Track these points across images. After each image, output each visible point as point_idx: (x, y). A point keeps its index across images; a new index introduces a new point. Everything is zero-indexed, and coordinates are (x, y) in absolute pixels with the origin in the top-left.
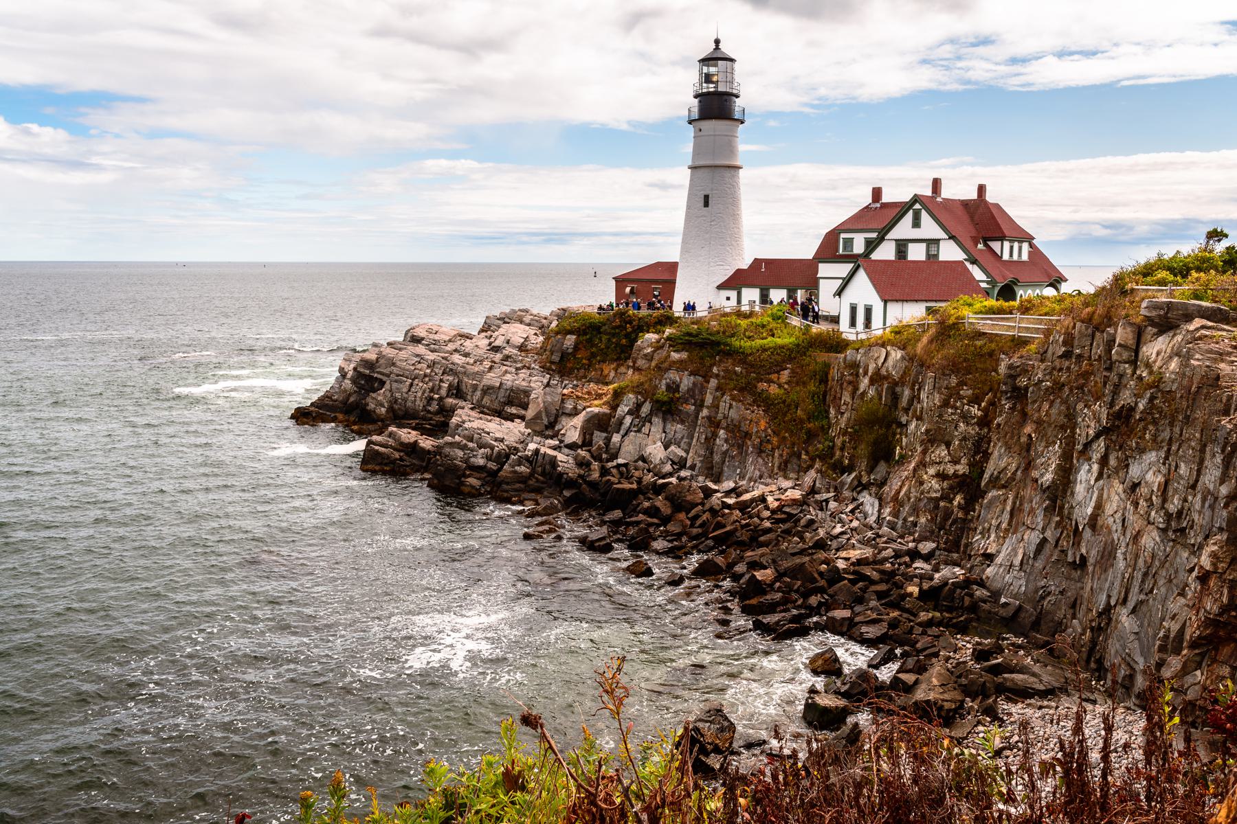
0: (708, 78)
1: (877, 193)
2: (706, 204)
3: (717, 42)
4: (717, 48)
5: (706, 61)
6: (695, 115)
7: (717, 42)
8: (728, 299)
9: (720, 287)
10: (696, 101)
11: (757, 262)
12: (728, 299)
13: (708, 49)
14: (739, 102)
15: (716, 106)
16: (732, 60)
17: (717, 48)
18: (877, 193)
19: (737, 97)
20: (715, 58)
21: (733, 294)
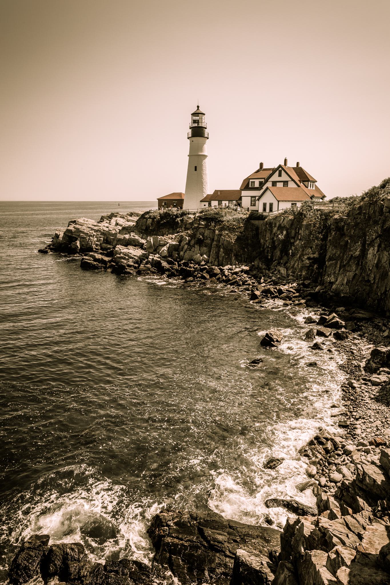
0: (195, 122)
1: (261, 165)
2: (196, 170)
3: (198, 107)
4: (198, 109)
5: (194, 114)
6: (190, 136)
7: (198, 107)
8: (205, 205)
10: (190, 130)
11: (216, 192)
12: (205, 205)
13: (194, 110)
15: (198, 132)
16: (204, 114)
17: (198, 109)
18: (261, 165)
19: (206, 128)
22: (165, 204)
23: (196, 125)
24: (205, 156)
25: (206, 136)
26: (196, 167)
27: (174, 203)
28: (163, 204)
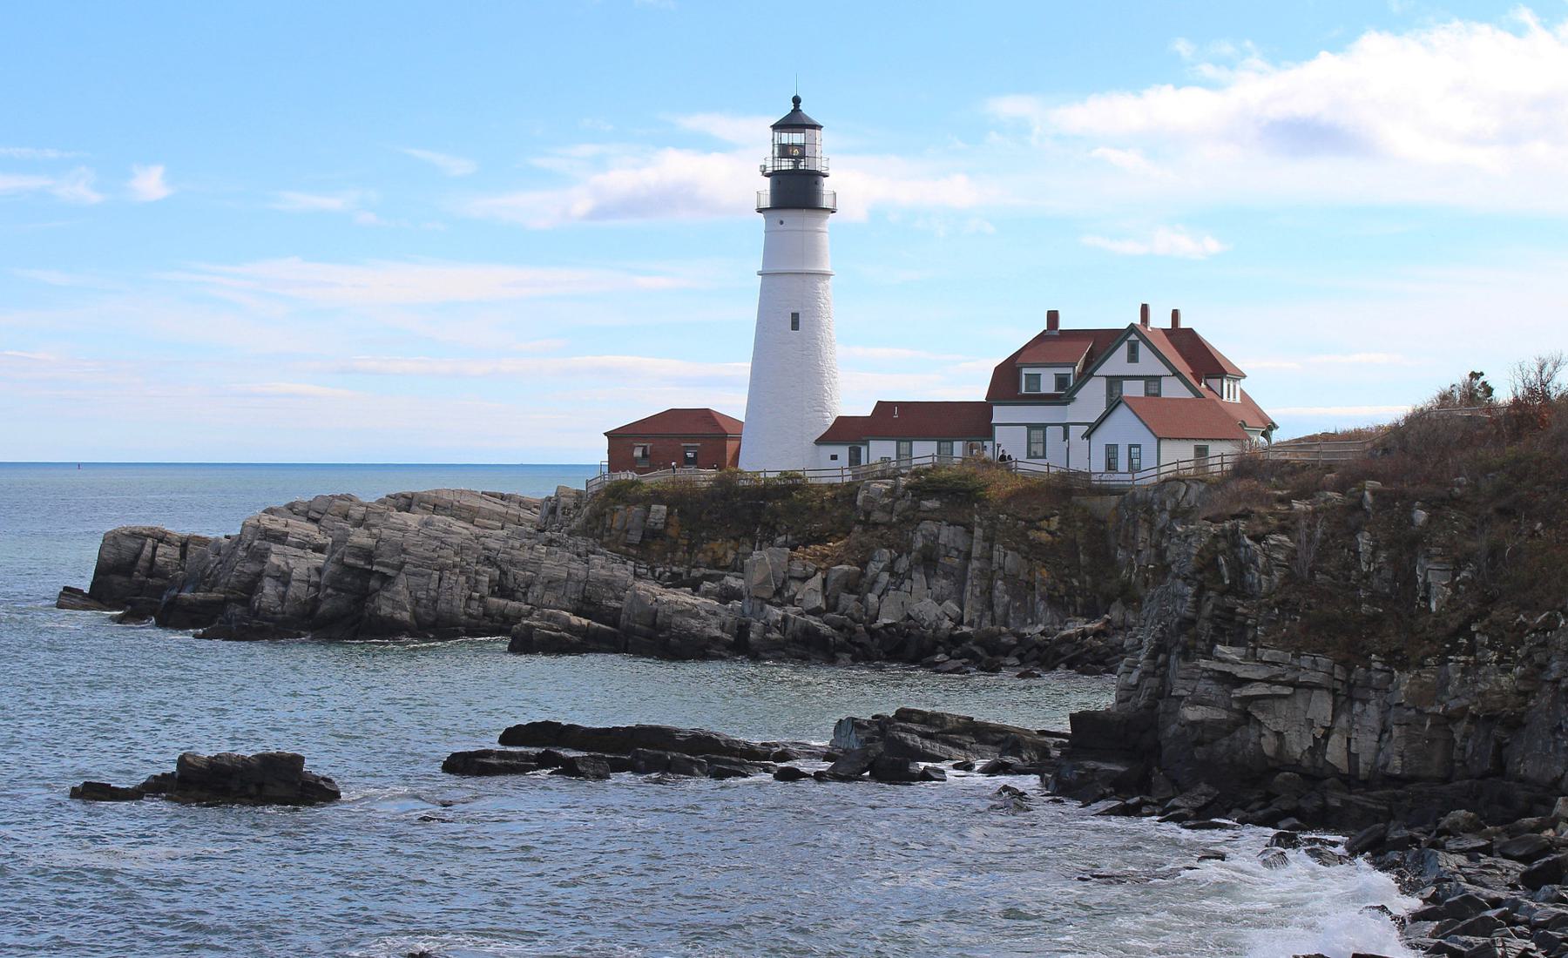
0: (785, 151)
1: (1053, 317)
2: (795, 325)
3: (796, 101)
4: (796, 109)
6: (766, 202)
7: (796, 101)
8: (834, 457)
9: (822, 441)
11: (882, 407)
12: (834, 457)
14: (827, 185)
15: (796, 190)
17: (796, 109)
18: (1053, 317)
19: (826, 176)
20: (794, 121)
21: (843, 452)
23: (786, 165)
24: (826, 275)
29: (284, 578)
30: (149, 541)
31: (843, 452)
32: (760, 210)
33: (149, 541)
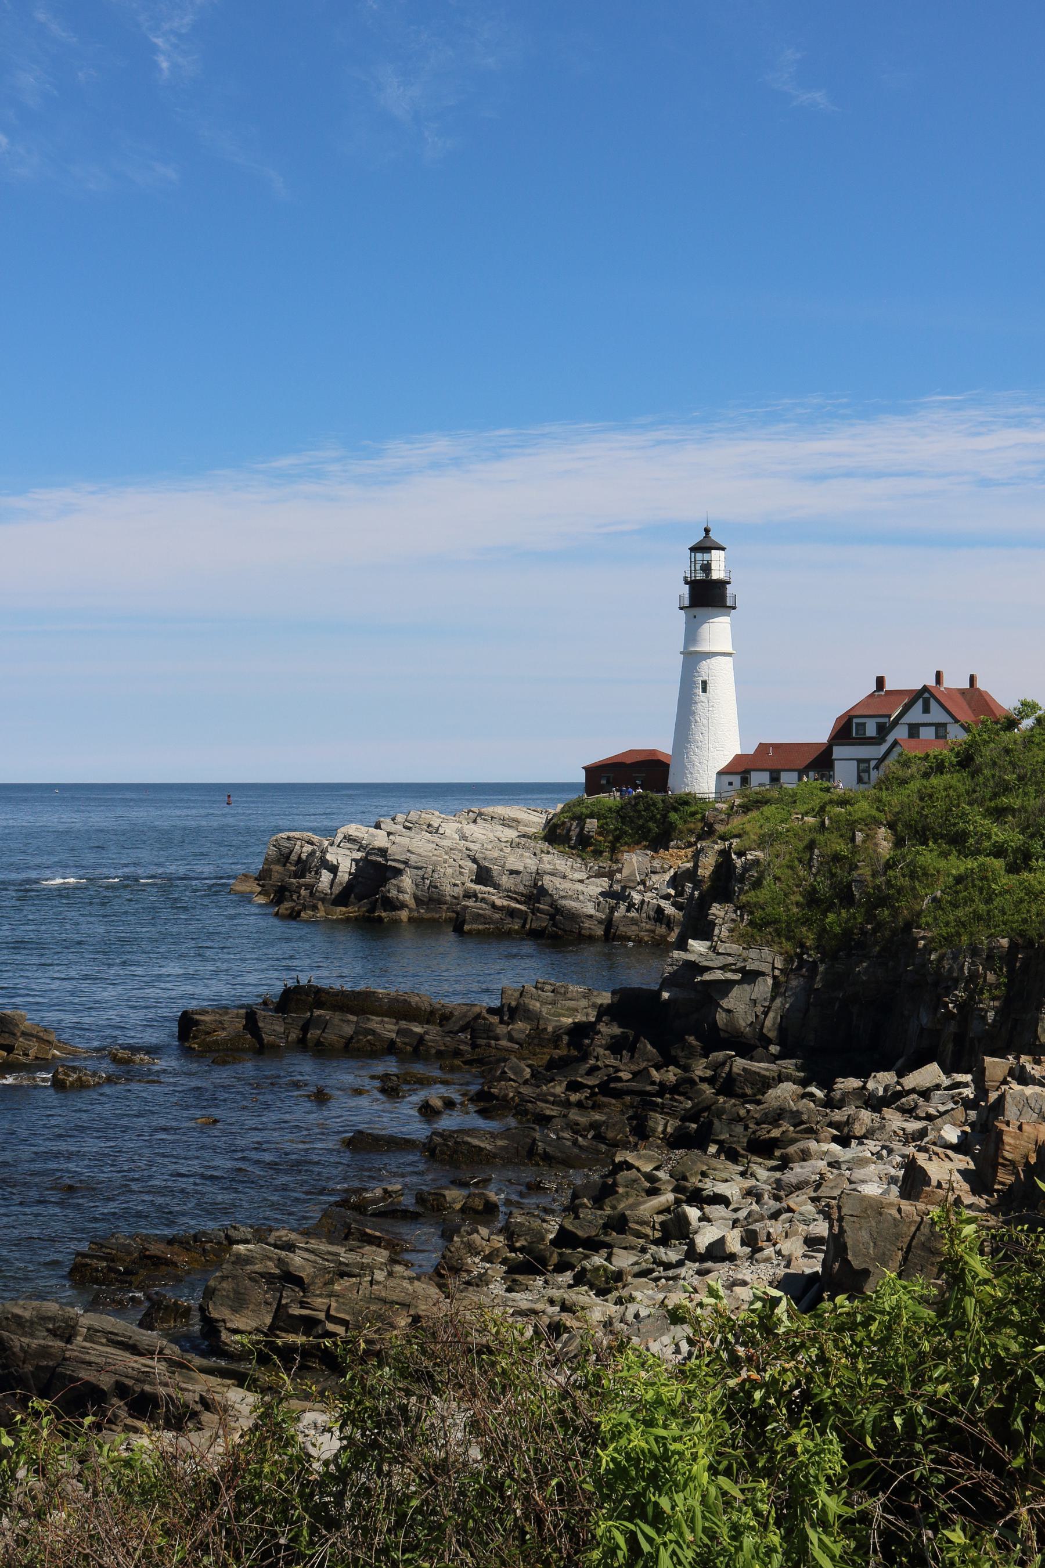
1: (880, 682)
2: (704, 690)
3: (707, 531)
5: (693, 549)
6: (687, 603)
7: (707, 531)
8: (731, 784)
11: (763, 748)
12: (731, 784)
13: (698, 537)
14: (730, 590)
15: (707, 595)
18: (880, 682)
19: (729, 583)
22: (608, 782)
23: (700, 575)
25: (729, 602)
26: (704, 683)
27: (637, 778)
28: (603, 782)
29: (334, 869)
30: (299, 843)
31: (737, 780)
32: (681, 608)
33: (299, 843)
